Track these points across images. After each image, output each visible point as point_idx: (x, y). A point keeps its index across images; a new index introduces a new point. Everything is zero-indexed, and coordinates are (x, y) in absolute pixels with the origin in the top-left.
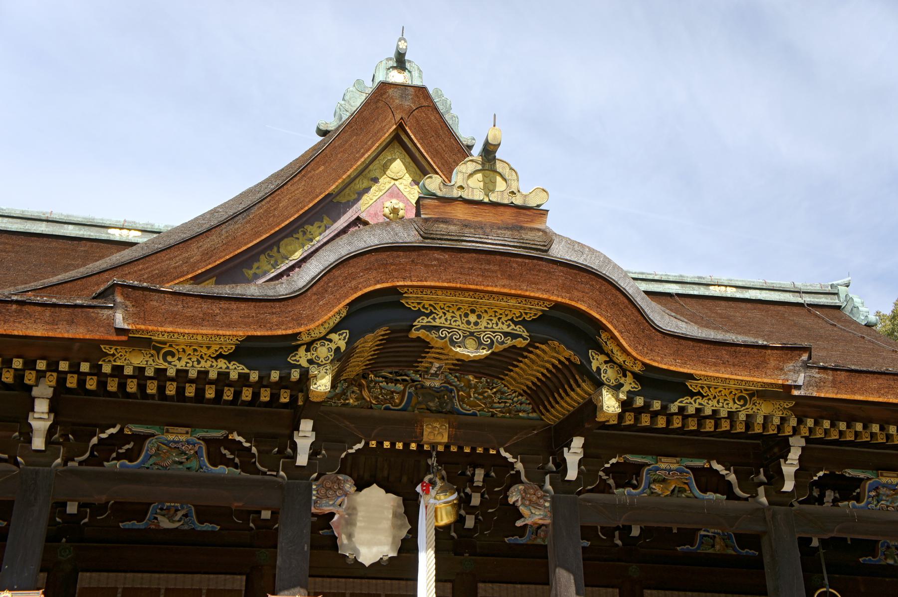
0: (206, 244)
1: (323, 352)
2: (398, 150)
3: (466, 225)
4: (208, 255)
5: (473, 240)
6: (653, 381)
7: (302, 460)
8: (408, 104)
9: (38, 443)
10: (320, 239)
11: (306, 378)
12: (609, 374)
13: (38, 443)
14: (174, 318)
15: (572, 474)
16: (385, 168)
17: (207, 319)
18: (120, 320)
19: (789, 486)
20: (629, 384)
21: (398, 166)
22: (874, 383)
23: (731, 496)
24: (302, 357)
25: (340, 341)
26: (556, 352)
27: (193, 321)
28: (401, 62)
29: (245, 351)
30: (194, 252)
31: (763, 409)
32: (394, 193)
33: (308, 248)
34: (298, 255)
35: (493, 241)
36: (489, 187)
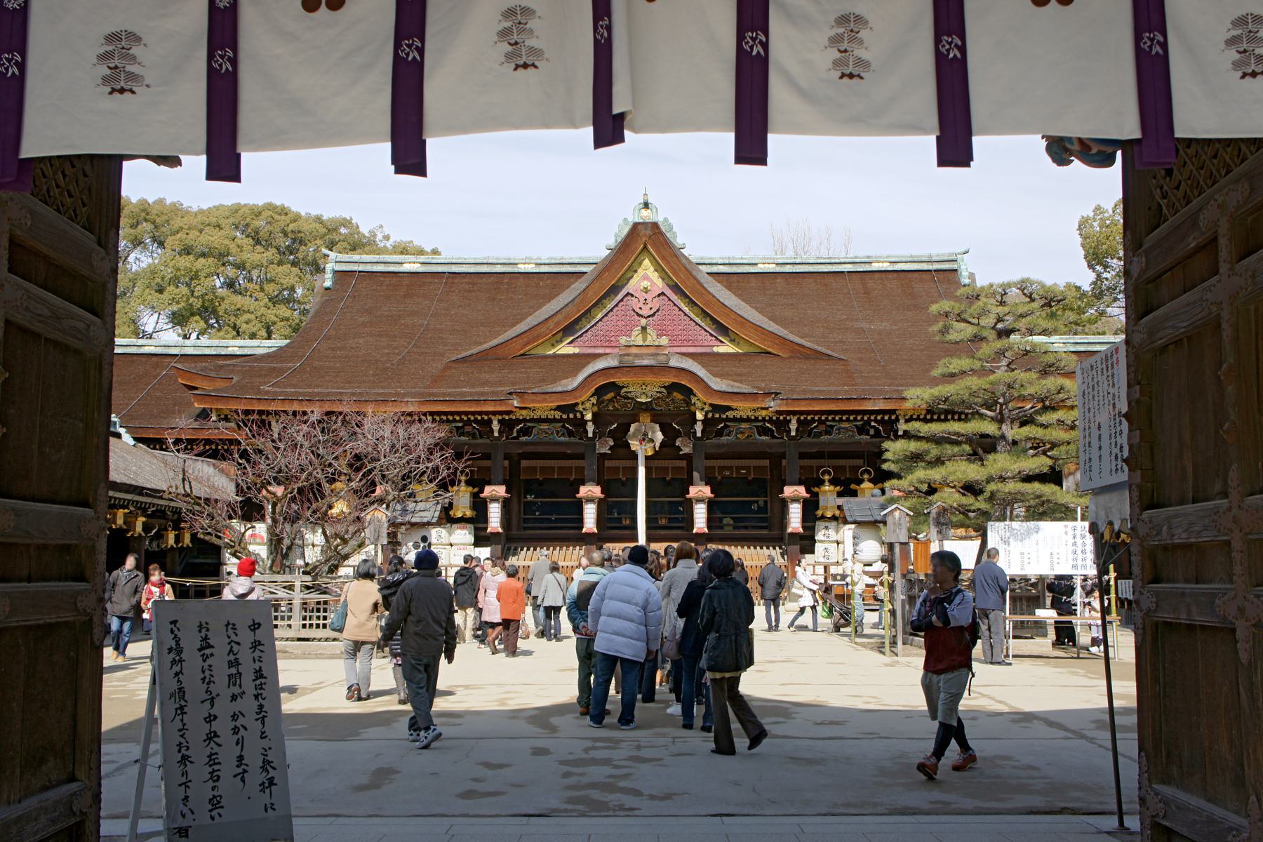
0: (556, 319)
1: (588, 405)
2: (645, 253)
3: (636, 355)
4: (557, 324)
5: (638, 362)
6: (715, 408)
7: (590, 435)
8: (649, 232)
9: (496, 434)
10: (610, 306)
11: (583, 416)
12: (699, 404)
13: (496, 434)
14: (533, 401)
15: (699, 434)
16: (640, 264)
17: (545, 400)
18: (516, 404)
19: (793, 433)
20: (707, 408)
21: (647, 262)
22: (803, 403)
23: (774, 437)
24: (580, 408)
25: (594, 400)
26: (678, 396)
27: (539, 402)
28: (646, 205)
29: (558, 408)
30: (551, 324)
31: (764, 413)
32: (646, 278)
33: (605, 311)
34: (600, 316)
35: (645, 362)
36: (644, 340)
